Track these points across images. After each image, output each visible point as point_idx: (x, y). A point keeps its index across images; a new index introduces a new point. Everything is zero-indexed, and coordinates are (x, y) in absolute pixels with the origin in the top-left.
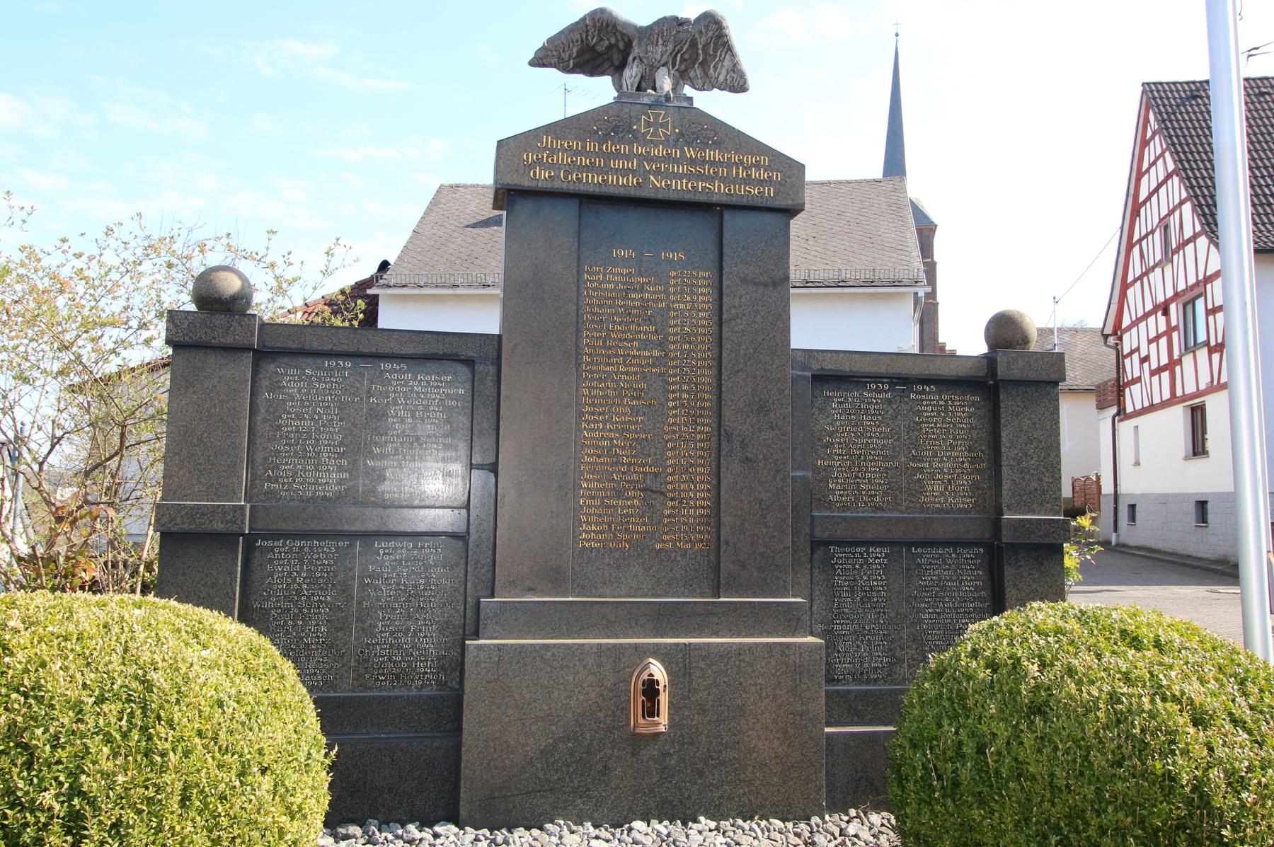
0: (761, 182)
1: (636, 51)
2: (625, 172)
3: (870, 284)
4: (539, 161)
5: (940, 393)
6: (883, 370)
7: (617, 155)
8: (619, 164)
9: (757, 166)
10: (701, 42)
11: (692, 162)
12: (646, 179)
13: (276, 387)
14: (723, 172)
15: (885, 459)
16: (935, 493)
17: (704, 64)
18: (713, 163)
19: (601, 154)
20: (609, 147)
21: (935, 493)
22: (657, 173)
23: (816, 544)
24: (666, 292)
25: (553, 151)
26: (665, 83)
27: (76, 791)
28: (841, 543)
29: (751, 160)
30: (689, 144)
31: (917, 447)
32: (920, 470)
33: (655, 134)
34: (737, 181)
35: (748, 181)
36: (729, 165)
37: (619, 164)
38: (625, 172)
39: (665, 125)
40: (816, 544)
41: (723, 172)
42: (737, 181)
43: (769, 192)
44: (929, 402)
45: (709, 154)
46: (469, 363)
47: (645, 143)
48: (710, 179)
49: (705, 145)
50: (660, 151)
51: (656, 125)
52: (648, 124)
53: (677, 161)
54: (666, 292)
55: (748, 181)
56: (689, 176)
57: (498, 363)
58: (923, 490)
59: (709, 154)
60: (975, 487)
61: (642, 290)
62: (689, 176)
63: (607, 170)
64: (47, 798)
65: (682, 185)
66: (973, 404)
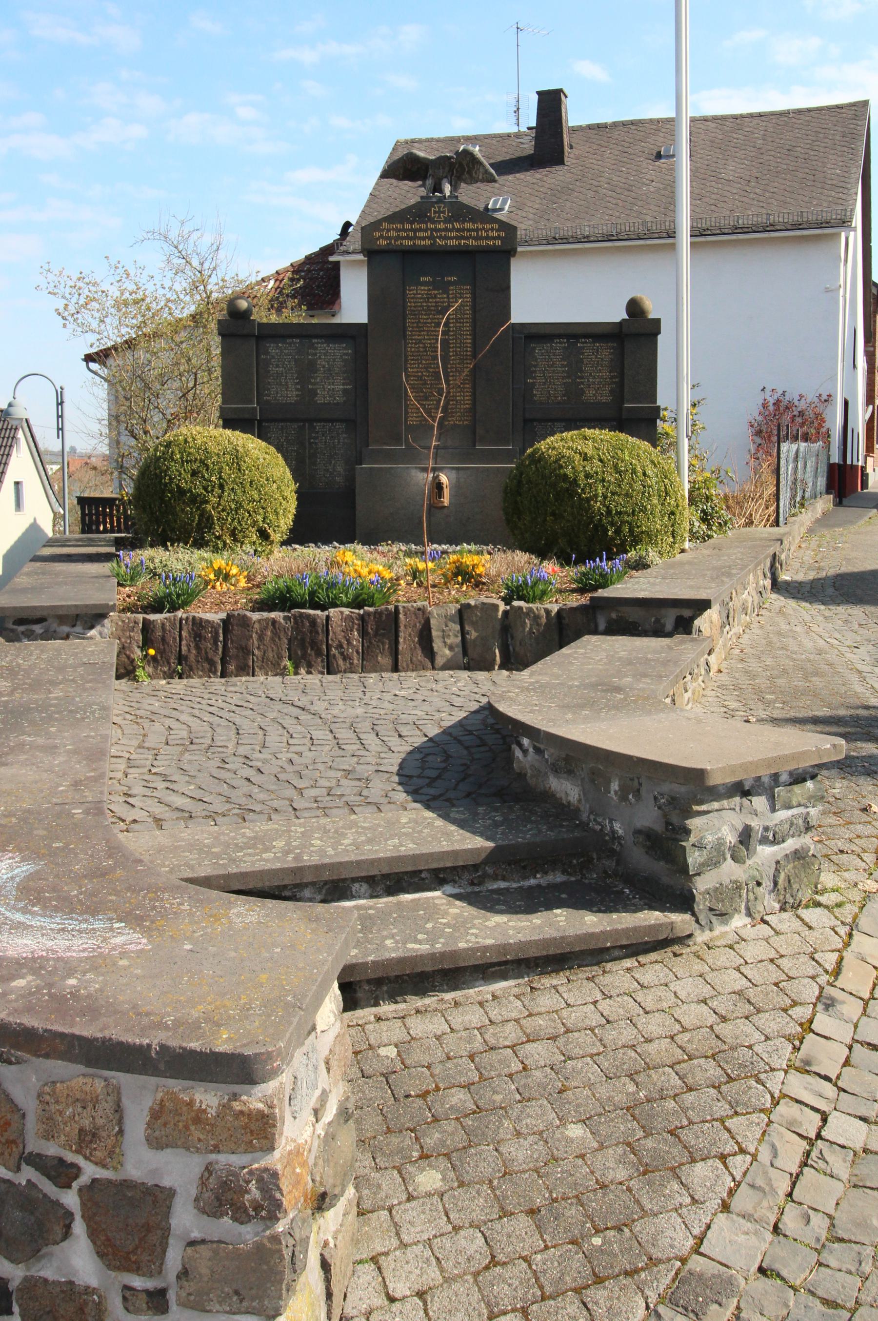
0: (494, 238)
1: (430, 172)
2: (424, 238)
3: (797, 226)
4: (381, 237)
5: (594, 342)
6: (562, 332)
7: (420, 230)
8: (421, 234)
9: (492, 229)
10: (464, 163)
11: (458, 230)
12: (435, 241)
13: (267, 353)
14: (474, 234)
15: (564, 378)
16: (590, 395)
17: (469, 173)
18: (469, 230)
19: (412, 230)
20: (416, 226)
21: (590, 395)
22: (440, 237)
23: (526, 421)
24: (448, 298)
25: (388, 230)
26: (447, 189)
27: (221, 477)
28: (540, 421)
29: (488, 226)
30: (456, 221)
31: (581, 371)
32: (582, 383)
33: (439, 217)
34: (482, 238)
35: (487, 238)
36: (477, 230)
37: (421, 234)
38: (424, 238)
39: (443, 212)
40: (526, 421)
41: (474, 234)
42: (482, 238)
43: (498, 243)
44: (588, 349)
45: (467, 225)
46: (353, 337)
47: (434, 222)
48: (467, 238)
49: (464, 221)
50: (441, 226)
51: (439, 212)
52: (435, 212)
53: (451, 230)
54: (448, 298)
55: (487, 238)
56: (457, 238)
57: (366, 337)
58: (583, 392)
59: (467, 225)
60: (612, 392)
61: (435, 297)
62: (457, 238)
63: (415, 238)
64: (213, 478)
65: (453, 242)
66: (612, 348)
